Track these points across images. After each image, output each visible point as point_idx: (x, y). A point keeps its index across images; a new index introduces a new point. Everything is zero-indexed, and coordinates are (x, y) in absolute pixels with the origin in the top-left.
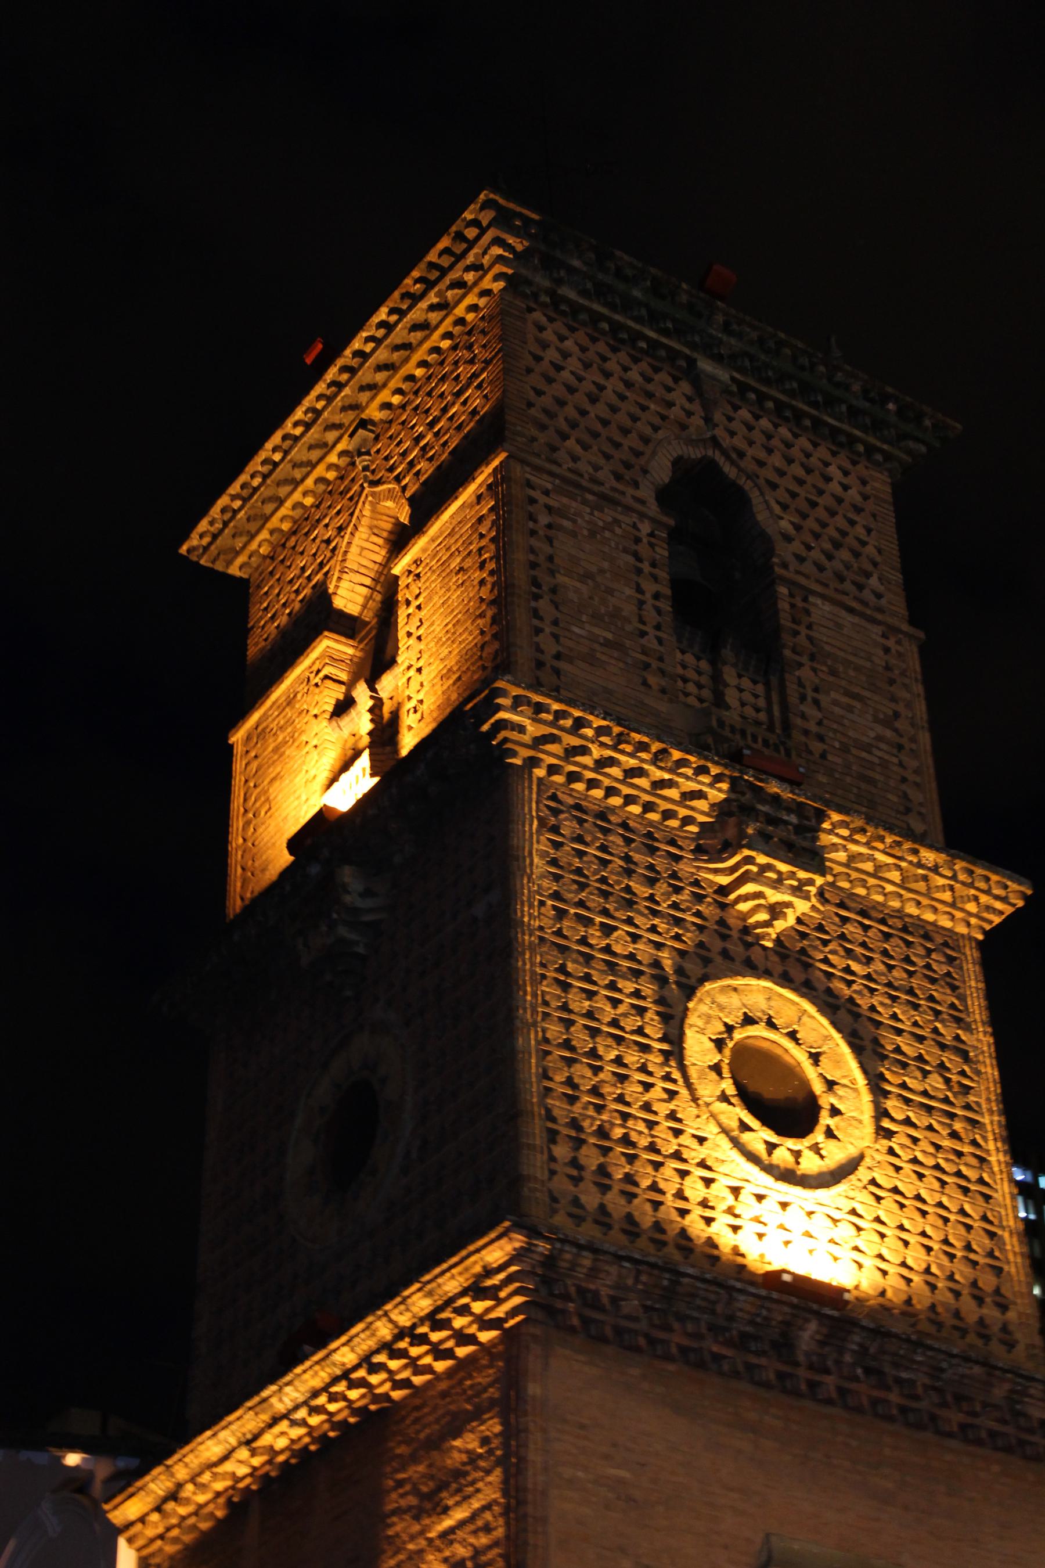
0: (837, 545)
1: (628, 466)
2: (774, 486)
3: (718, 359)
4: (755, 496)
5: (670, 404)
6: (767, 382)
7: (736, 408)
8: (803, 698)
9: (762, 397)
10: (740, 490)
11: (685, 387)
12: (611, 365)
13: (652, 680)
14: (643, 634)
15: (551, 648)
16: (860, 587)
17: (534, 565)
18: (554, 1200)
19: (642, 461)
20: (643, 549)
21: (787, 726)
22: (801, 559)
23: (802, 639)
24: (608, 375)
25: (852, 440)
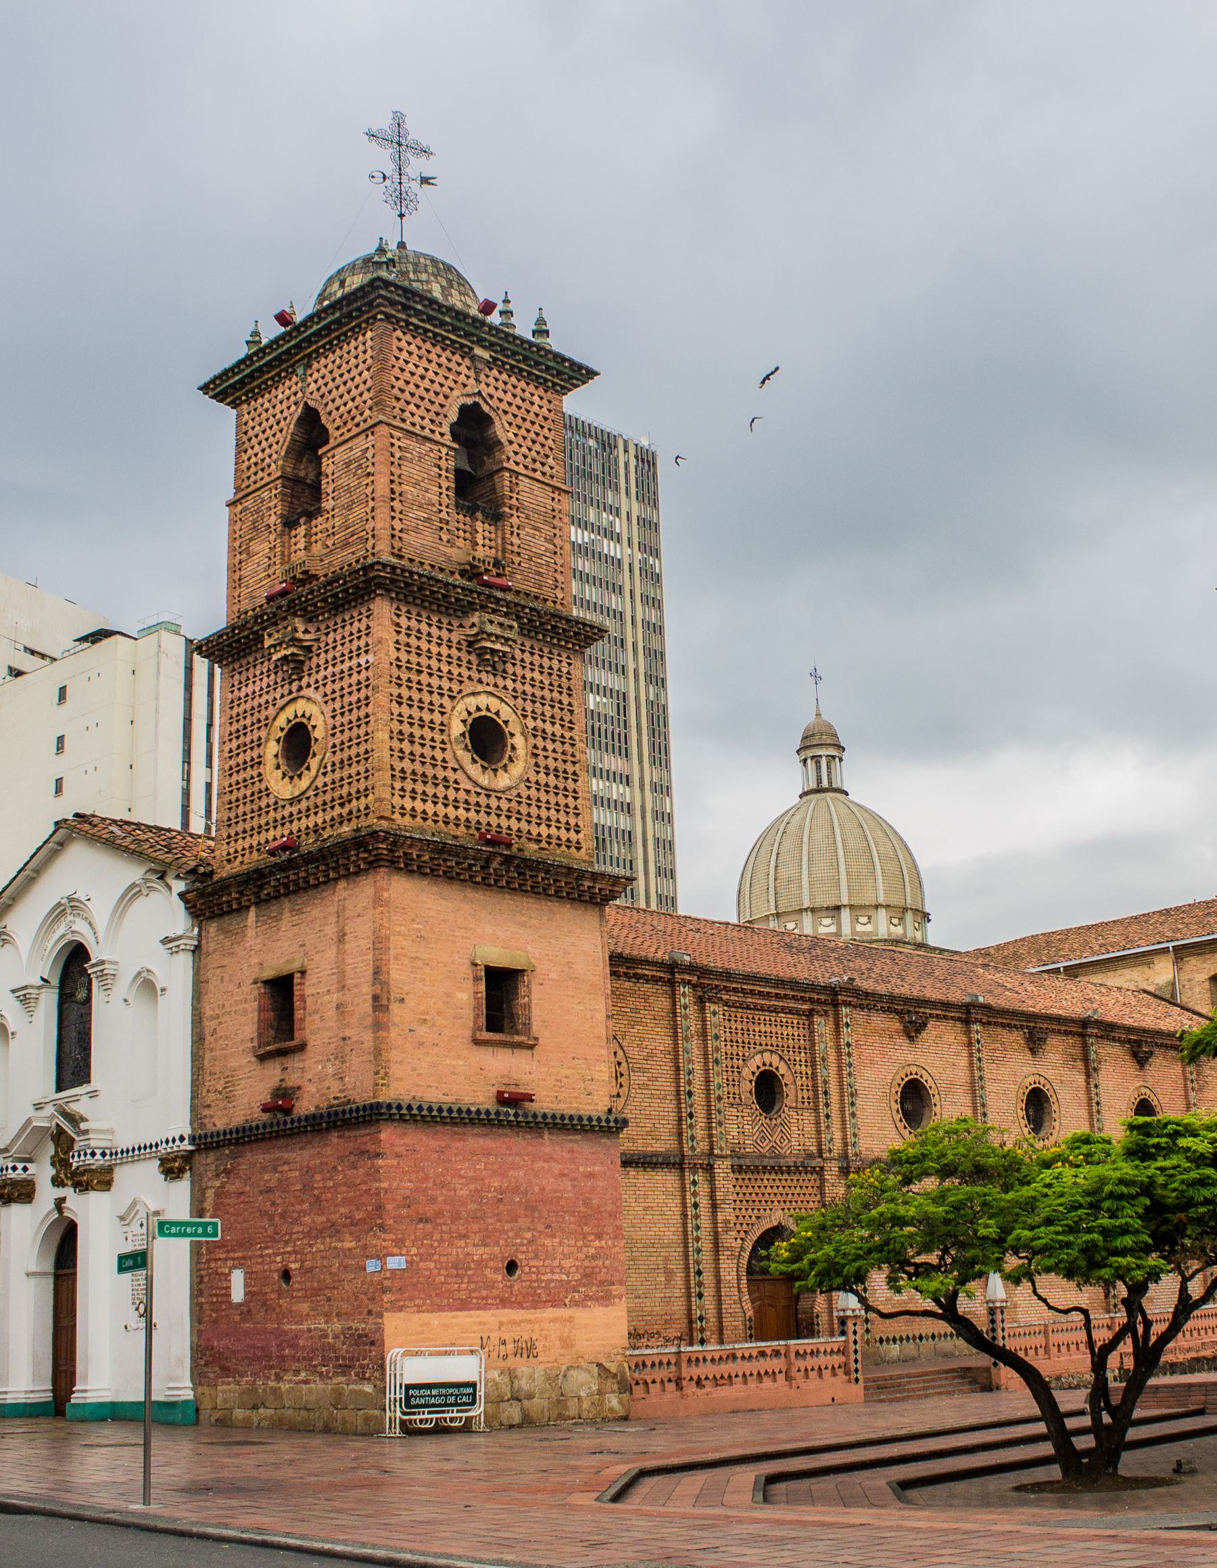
0: (534, 442)
1: (437, 414)
2: (506, 412)
3: (484, 347)
4: (496, 420)
5: (459, 374)
6: (507, 357)
7: (491, 369)
8: (512, 533)
9: (504, 363)
10: (491, 419)
11: (467, 362)
12: (433, 356)
13: (445, 537)
14: (441, 511)
15: (398, 525)
16: (543, 464)
17: (392, 482)
18: (394, 807)
19: (445, 409)
20: (443, 463)
21: (504, 551)
22: (516, 453)
23: (514, 502)
24: (430, 361)
25: (546, 380)
